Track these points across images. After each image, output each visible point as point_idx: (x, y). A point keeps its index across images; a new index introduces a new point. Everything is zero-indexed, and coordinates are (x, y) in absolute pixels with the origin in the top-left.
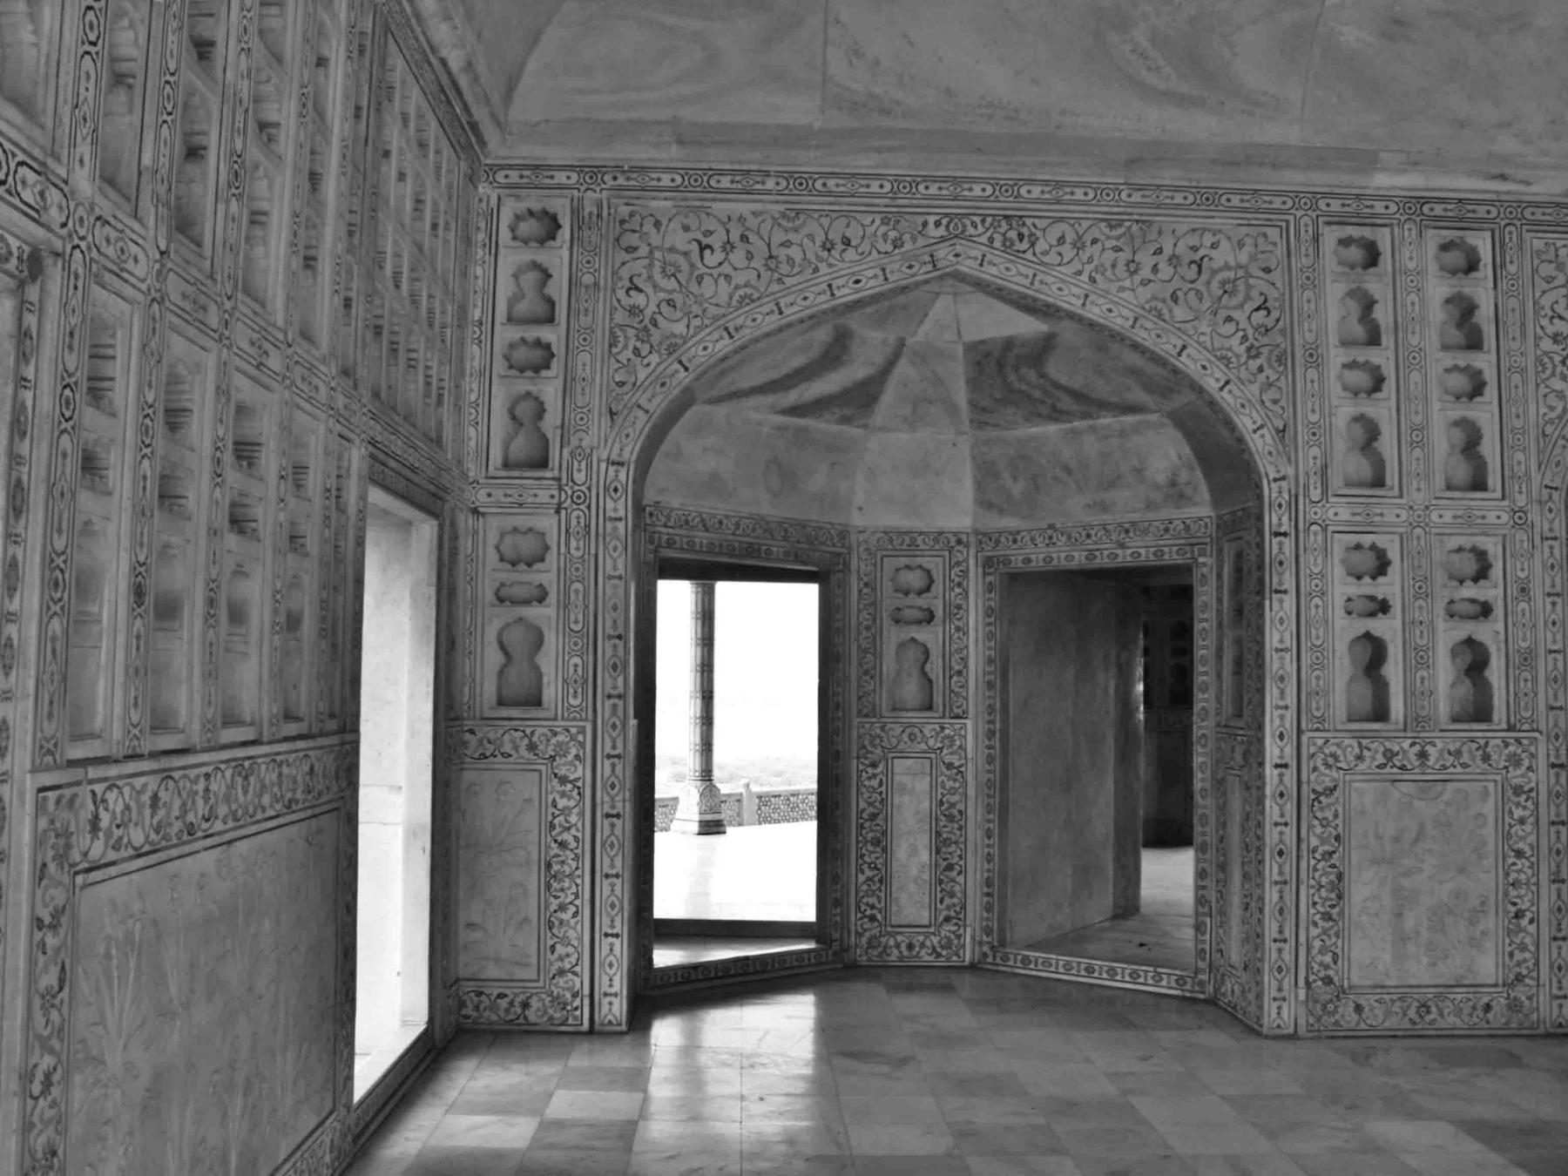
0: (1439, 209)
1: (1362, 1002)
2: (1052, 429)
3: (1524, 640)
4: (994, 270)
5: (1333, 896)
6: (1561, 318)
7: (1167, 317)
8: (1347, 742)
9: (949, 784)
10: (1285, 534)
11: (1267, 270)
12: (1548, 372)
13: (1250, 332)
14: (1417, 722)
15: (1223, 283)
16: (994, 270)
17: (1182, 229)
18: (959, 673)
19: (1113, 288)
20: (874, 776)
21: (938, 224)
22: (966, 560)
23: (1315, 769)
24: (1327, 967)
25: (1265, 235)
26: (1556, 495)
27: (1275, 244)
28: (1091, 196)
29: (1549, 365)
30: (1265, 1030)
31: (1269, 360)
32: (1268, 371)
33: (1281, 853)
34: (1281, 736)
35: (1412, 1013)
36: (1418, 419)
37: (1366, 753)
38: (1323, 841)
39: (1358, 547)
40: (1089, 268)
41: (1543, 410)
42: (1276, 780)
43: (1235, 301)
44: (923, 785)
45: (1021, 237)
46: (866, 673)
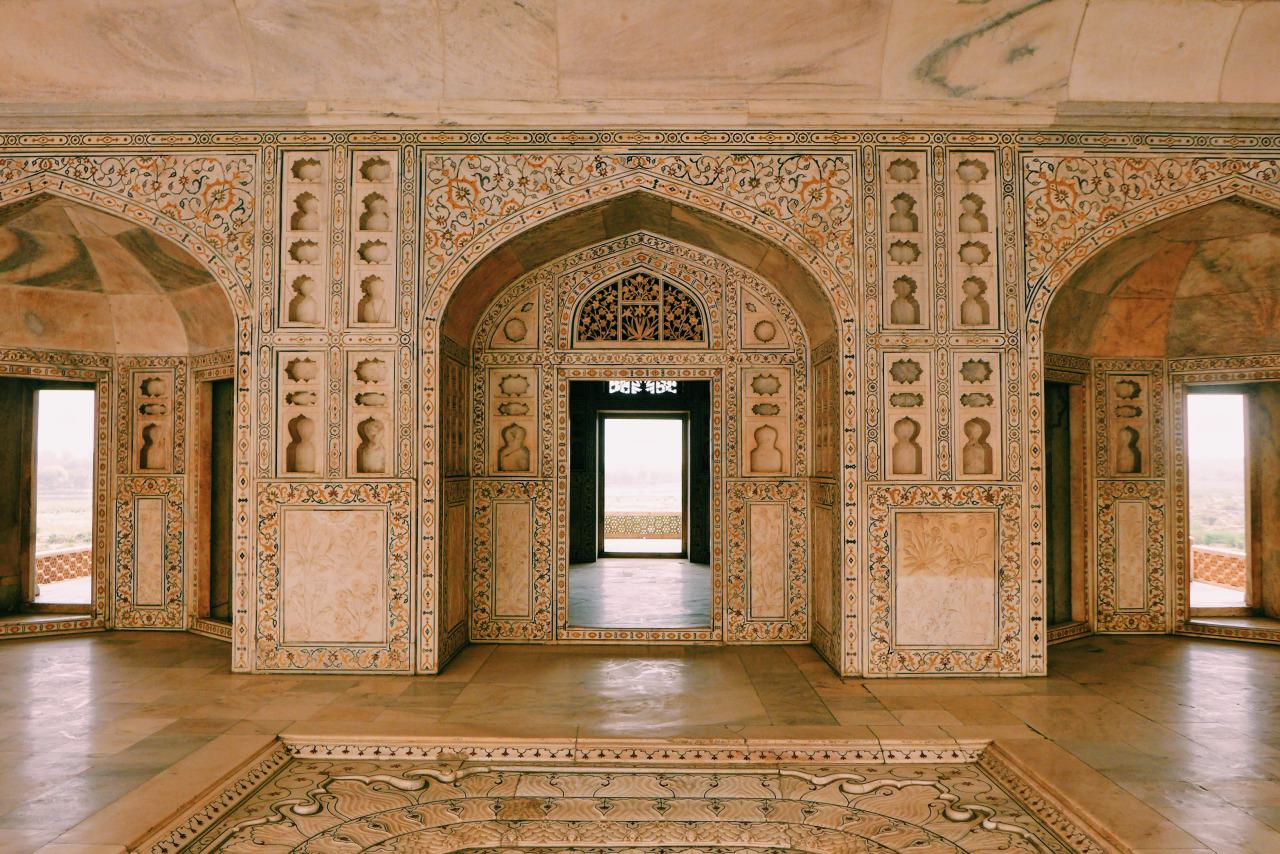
0: (360, 138)
1: (291, 650)
2: (194, 290)
3: (405, 419)
4: (68, 191)
5: (273, 583)
6: (443, 207)
7: (176, 217)
8: (283, 485)
9: (173, 515)
10: (248, 353)
11: (244, 184)
12: (433, 243)
13: (231, 224)
14: (331, 471)
15: (214, 194)
16: (68, 191)
17: (189, 160)
18: (180, 445)
19: (143, 199)
20: (127, 510)
21: (34, 163)
22: (186, 374)
23: (262, 502)
24: (269, 629)
25: (245, 161)
26: (433, 324)
27: (251, 166)
28: (129, 140)
29: (434, 238)
30: (234, 669)
31: (242, 242)
32: (241, 249)
33: (242, 556)
34: (243, 481)
35: (325, 659)
36: (338, 277)
37: (295, 492)
38: (267, 548)
39: (297, 360)
40: (128, 188)
41: (427, 268)
42: (240, 509)
43: (223, 204)
44: (157, 516)
45: (86, 169)
46: (122, 445)
